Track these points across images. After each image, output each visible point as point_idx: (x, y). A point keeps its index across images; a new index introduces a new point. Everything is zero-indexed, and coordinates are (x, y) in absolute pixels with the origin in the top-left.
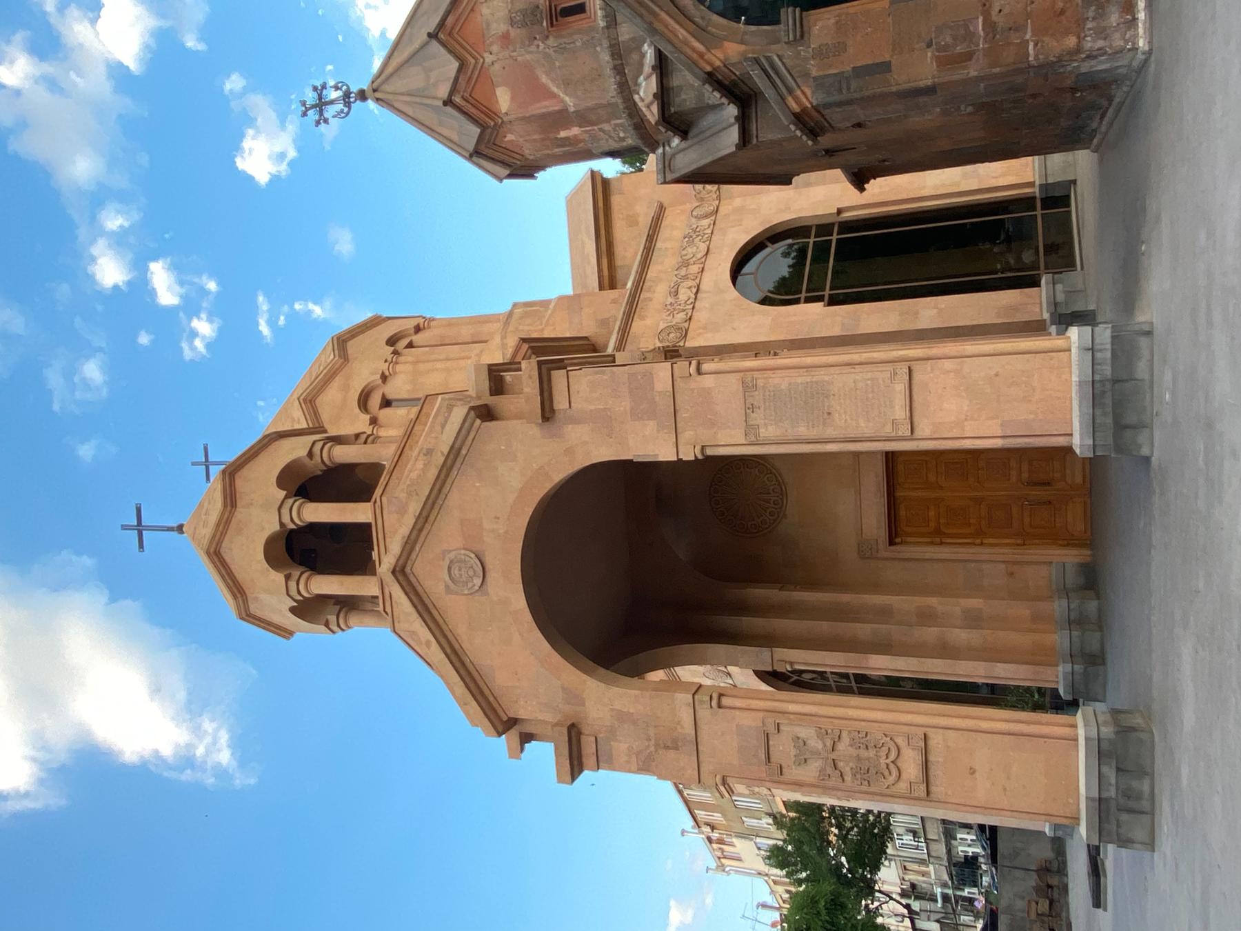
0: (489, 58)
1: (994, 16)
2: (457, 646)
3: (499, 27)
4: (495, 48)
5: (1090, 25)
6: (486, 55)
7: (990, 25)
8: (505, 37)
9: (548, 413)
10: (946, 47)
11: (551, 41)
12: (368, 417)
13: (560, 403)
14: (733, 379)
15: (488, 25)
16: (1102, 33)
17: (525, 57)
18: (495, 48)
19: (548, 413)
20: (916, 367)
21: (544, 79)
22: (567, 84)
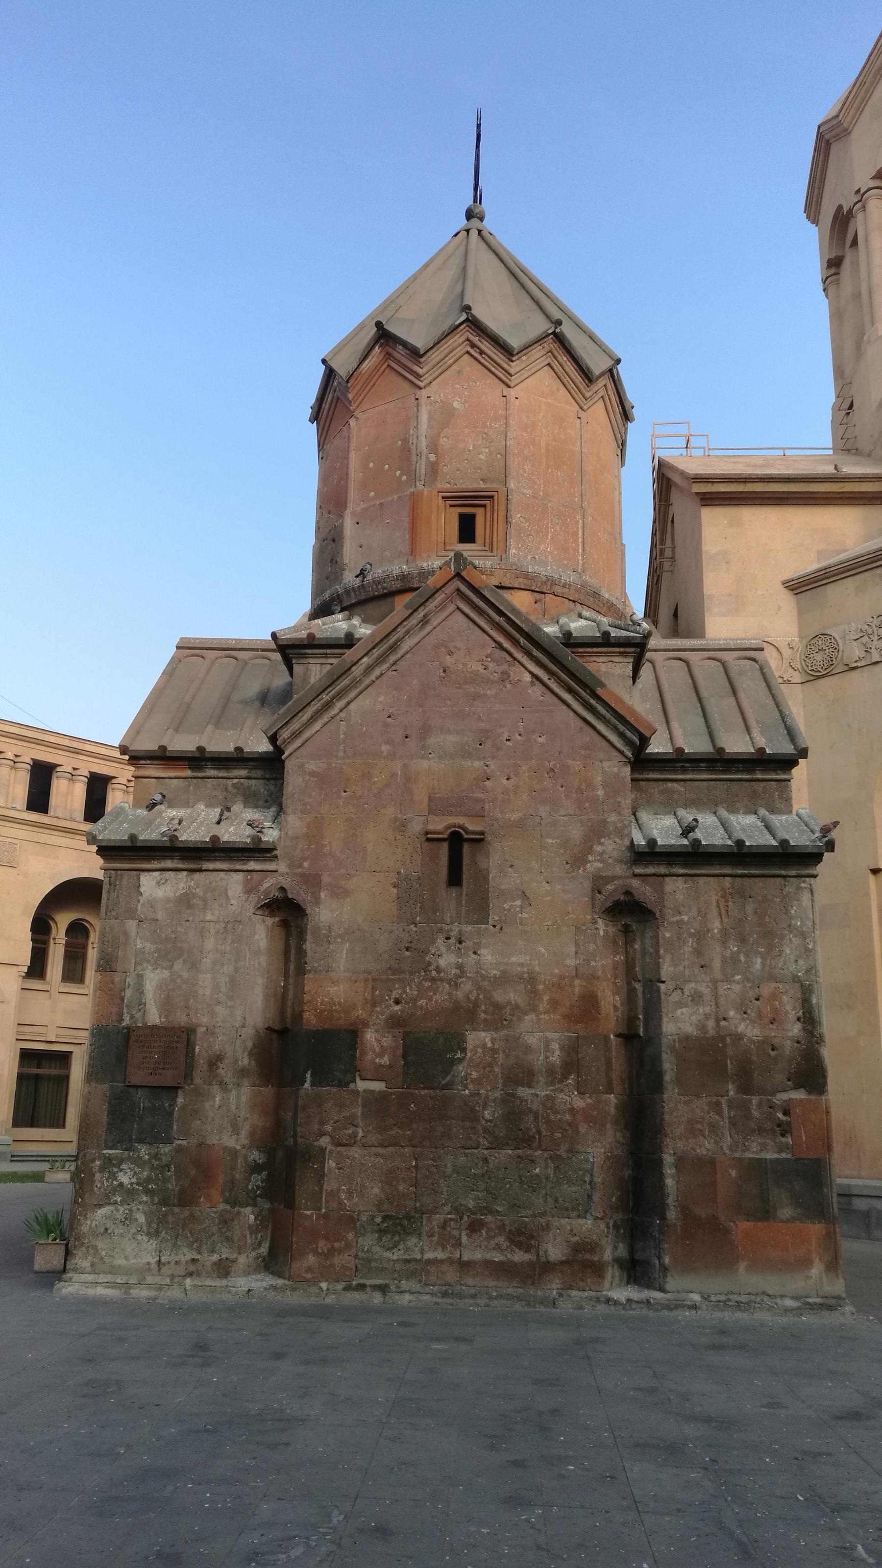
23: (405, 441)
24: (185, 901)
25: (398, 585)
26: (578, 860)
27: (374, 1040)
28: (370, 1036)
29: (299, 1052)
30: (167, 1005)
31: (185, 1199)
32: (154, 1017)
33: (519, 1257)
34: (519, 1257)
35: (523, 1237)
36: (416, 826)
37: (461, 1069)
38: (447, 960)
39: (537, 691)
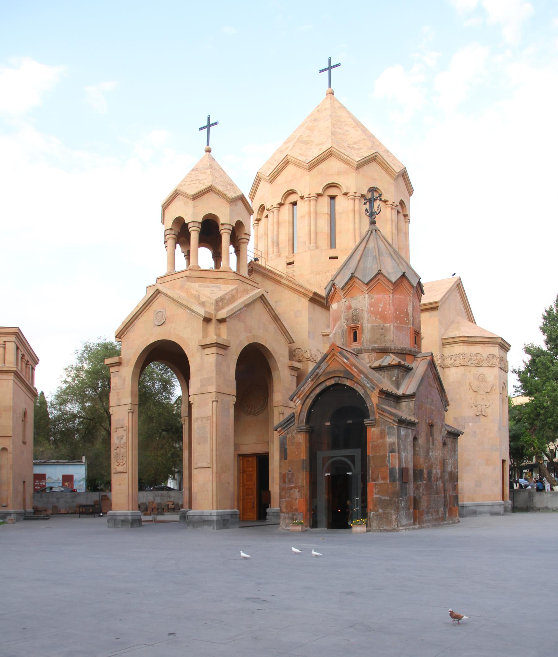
0: (344, 300)
1: (293, 490)
2: (139, 317)
3: (355, 304)
4: (347, 303)
5: (287, 515)
6: (345, 300)
7: (291, 489)
8: (350, 307)
9: (204, 347)
10: (288, 476)
11: (346, 327)
12: (321, 192)
13: (207, 351)
14: (210, 413)
15: (355, 299)
16: (285, 518)
17: (343, 315)
18: (347, 303)
19: (204, 347)
20: (210, 470)
21: (337, 324)
22: (335, 334)
23: (407, 310)
24: (406, 435)
25: (409, 352)
26: (441, 433)
27: (425, 471)
28: (424, 470)
29: (418, 474)
30: (406, 463)
31: (409, 509)
32: (404, 466)
33: (437, 516)
34: (437, 516)
35: (437, 512)
36: (427, 422)
37: (433, 478)
38: (431, 454)
39: (437, 391)
